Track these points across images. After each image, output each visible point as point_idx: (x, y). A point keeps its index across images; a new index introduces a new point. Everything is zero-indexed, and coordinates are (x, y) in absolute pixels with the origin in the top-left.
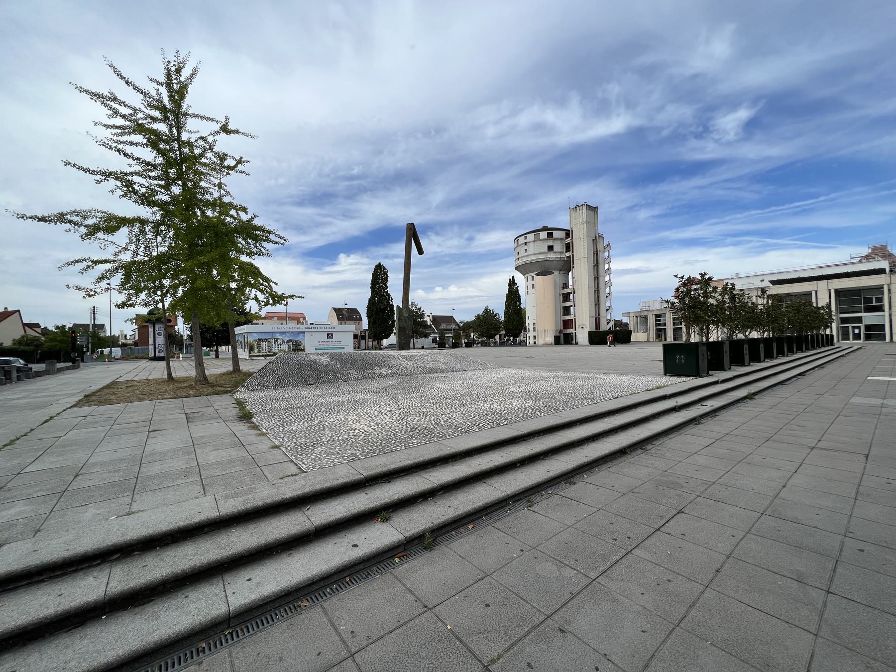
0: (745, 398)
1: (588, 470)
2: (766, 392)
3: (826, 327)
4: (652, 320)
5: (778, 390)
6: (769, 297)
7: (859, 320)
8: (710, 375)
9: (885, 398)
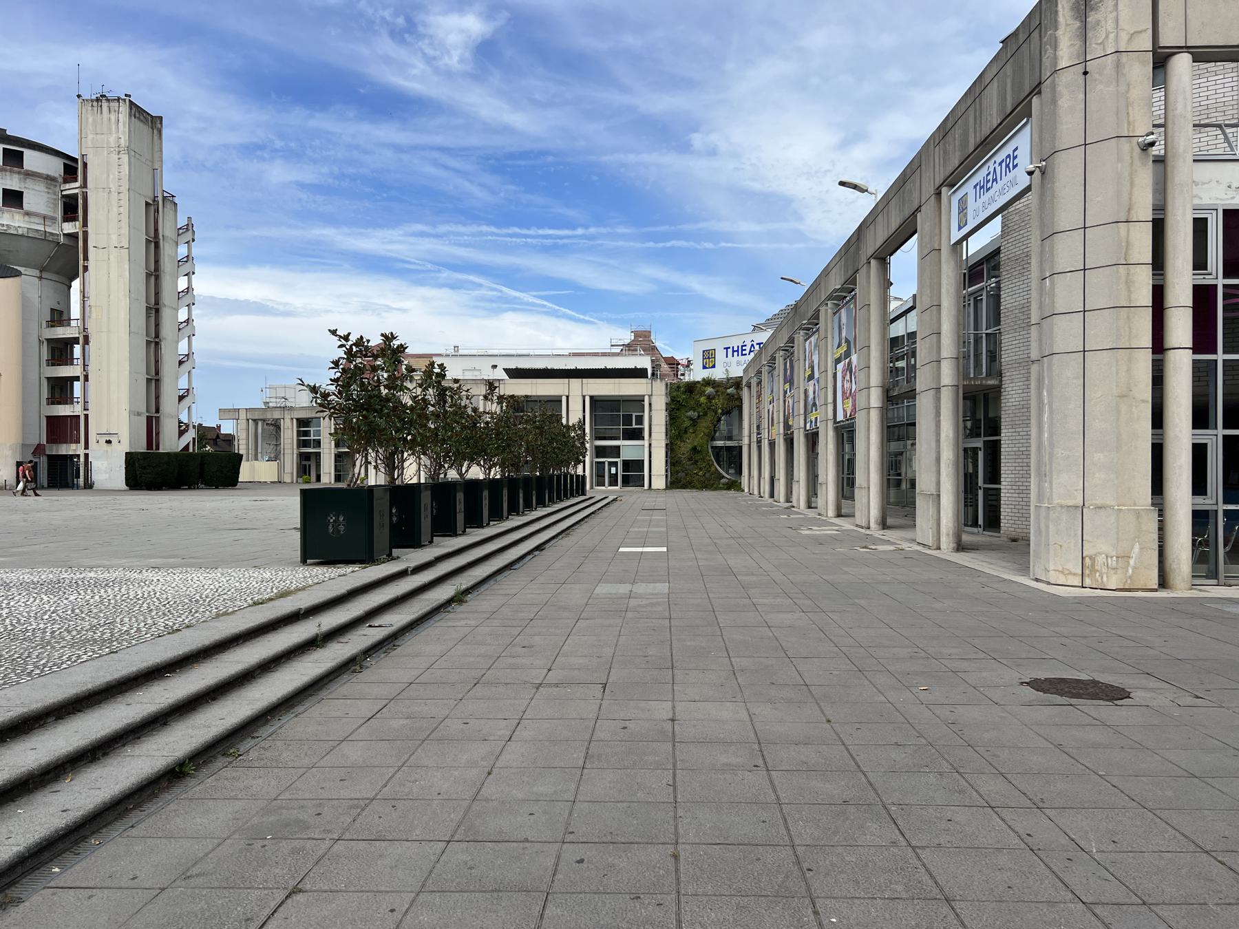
0: (449, 602)
1: (66, 850)
2: (486, 586)
3: (578, 462)
4: (290, 431)
5: (505, 579)
6: (501, 398)
7: (616, 451)
8: (393, 559)
9: (633, 583)
